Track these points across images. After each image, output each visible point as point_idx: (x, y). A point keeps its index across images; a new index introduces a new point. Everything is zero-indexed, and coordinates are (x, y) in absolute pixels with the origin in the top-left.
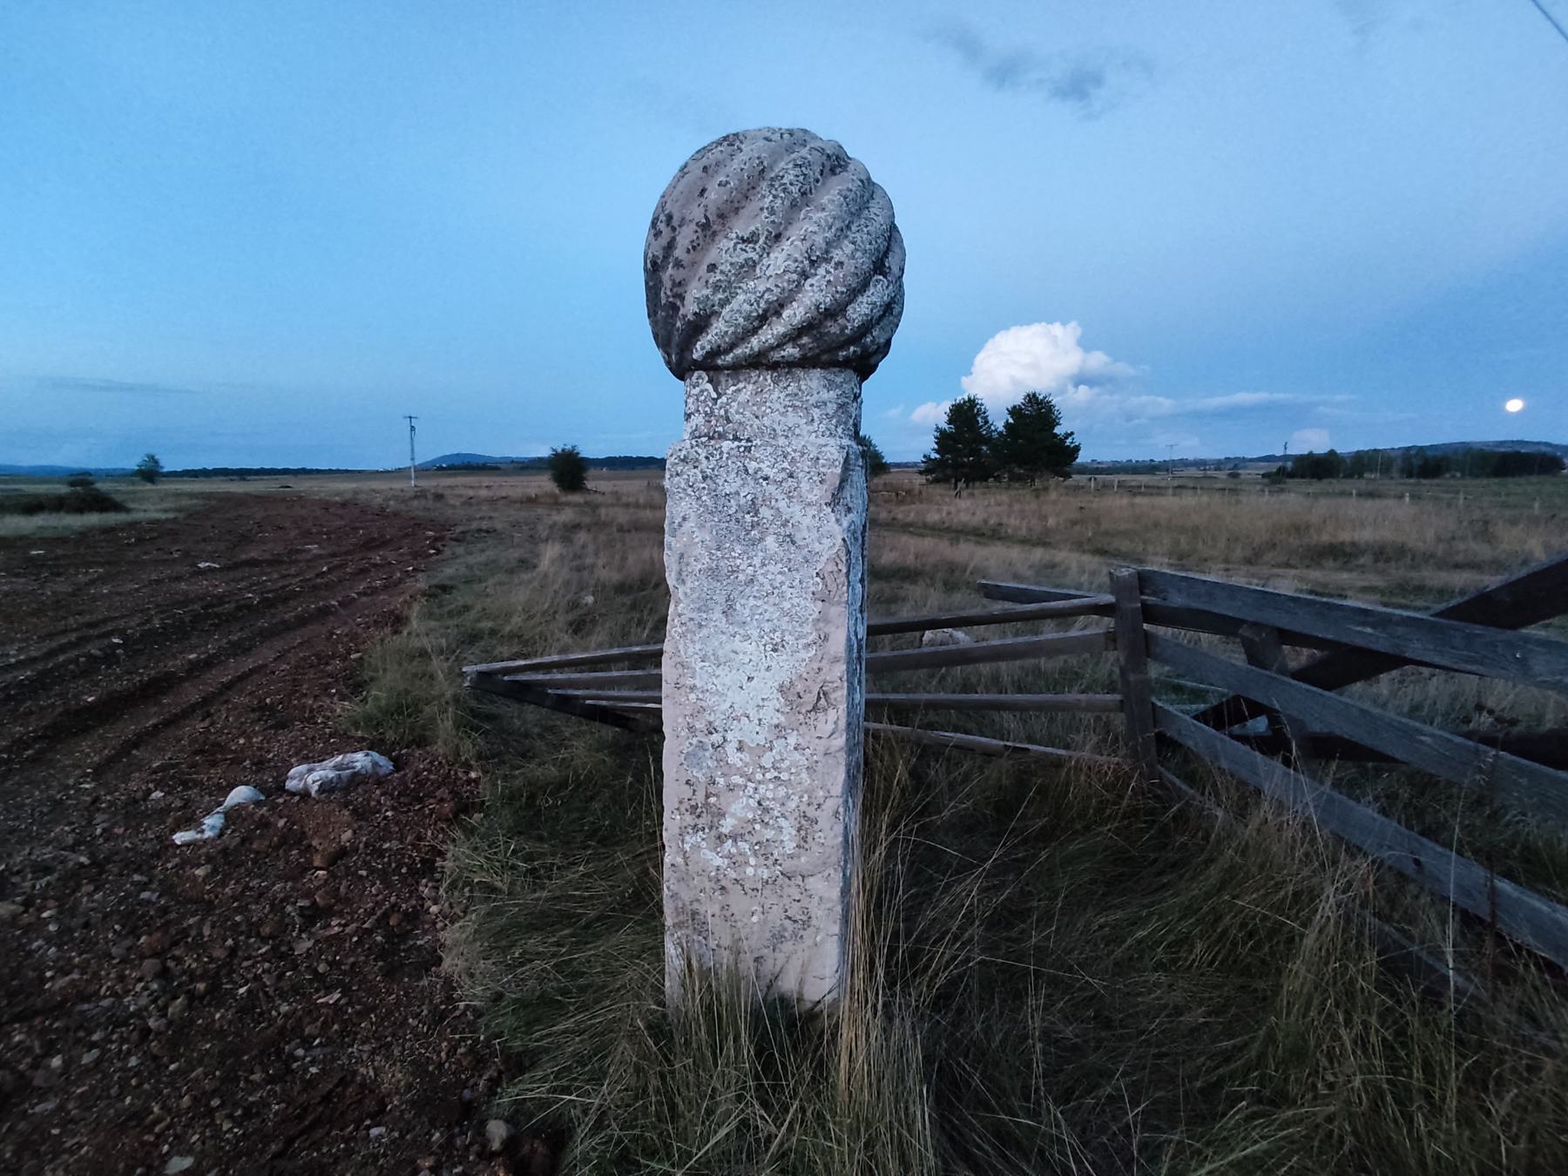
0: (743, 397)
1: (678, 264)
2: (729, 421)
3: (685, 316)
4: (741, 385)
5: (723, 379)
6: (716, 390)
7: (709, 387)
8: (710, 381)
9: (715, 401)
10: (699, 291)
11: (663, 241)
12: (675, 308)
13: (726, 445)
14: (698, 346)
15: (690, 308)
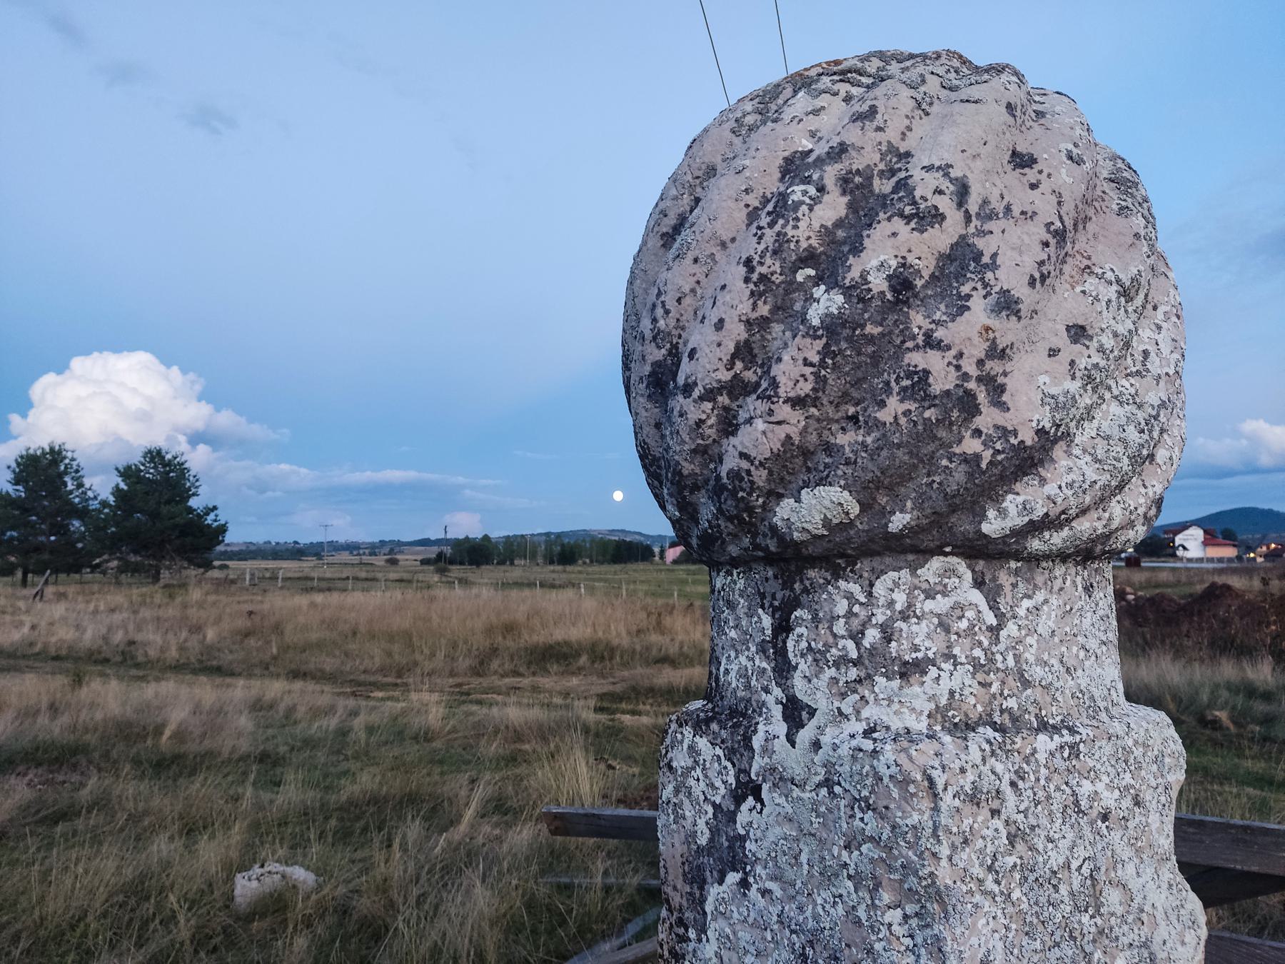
0: (1046, 623)
1: (1007, 305)
2: (1026, 684)
3: (1005, 433)
4: (1040, 596)
5: (1005, 579)
6: (994, 607)
7: (977, 597)
8: (979, 584)
9: (995, 631)
10: (1056, 380)
11: (941, 238)
12: (969, 406)
13: (1044, 743)
14: (1011, 503)
15: (1026, 413)
